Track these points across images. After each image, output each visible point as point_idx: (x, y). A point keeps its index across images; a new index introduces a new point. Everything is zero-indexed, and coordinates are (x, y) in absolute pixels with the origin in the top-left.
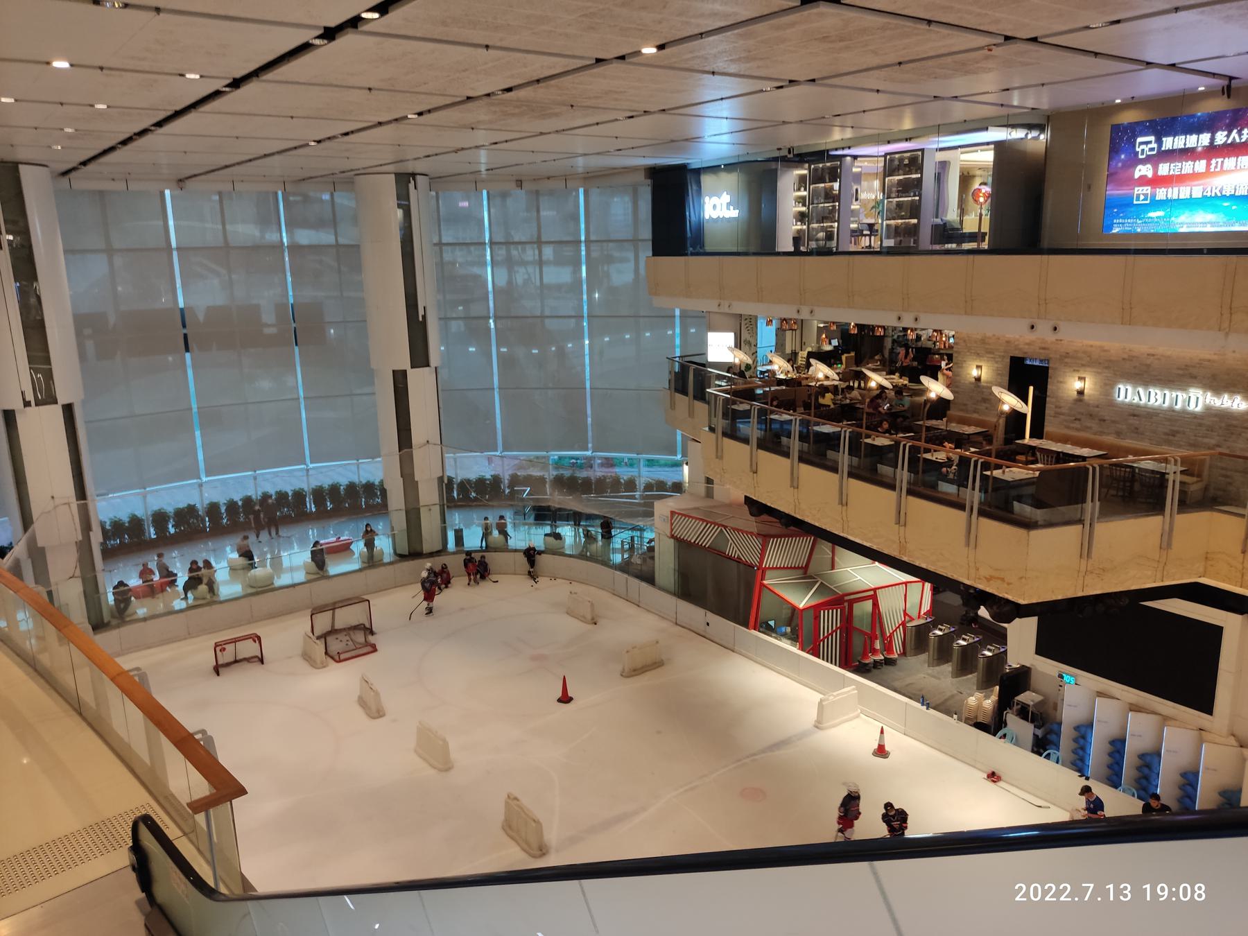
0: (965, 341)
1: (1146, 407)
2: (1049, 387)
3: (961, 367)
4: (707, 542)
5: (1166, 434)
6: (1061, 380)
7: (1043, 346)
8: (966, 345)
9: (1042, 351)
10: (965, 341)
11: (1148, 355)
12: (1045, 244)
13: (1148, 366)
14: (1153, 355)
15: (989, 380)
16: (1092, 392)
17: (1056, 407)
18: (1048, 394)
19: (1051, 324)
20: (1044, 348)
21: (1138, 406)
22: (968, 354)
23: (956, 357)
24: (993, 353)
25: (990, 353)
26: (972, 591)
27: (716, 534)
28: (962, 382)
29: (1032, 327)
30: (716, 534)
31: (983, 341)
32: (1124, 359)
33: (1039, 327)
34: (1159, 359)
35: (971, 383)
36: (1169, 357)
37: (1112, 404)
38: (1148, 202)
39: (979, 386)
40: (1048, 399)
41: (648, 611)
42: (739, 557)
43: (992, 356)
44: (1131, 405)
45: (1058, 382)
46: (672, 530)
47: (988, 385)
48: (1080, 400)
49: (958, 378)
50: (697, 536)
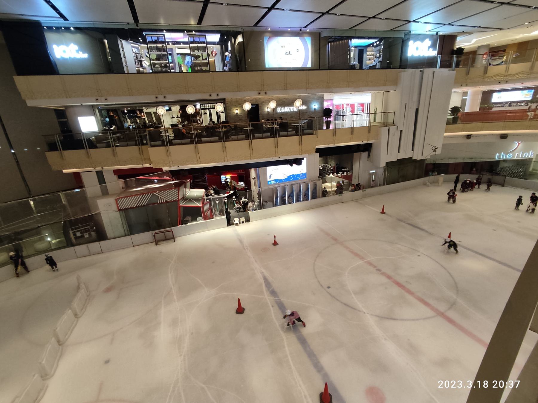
0: (230, 102)
1: (285, 112)
2: (259, 112)
3: (231, 111)
4: (145, 203)
5: (291, 118)
6: (262, 109)
7: (256, 100)
8: (231, 103)
9: (256, 102)
10: (230, 102)
11: (284, 99)
12: (247, 70)
13: (284, 102)
14: (285, 99)
15: (241, 113)
16: (271, 111)
17: (262, 117)
18: (260, 114)
19: (264, 92)
20: (256, 101)
21: (283, 112)
22: (232, 106)
23: (174, 122)
24: (241, 105)
25: (240, 105)
26: (293, 160)
27: (150, 197)
28: (232, 115)
29: (259, 93)
30: (150, 197)
31: (237, 101)
32: (278, 101)
33: (261, 93)
34: (286, 100)
35: (235, 115)
36: (288, 99)
37: (277, 113)
38: (355, 42)
39: (238, 116)
40: (260, 115)
41: (111, 251)
42: (166, 201)
43: (240, 105)
44: (281, 112)
45: (262, 110)
46: (118, 207)
47: (241, 115)
48: (269, 114)
49: (230, 114)
50: (137, 203)
